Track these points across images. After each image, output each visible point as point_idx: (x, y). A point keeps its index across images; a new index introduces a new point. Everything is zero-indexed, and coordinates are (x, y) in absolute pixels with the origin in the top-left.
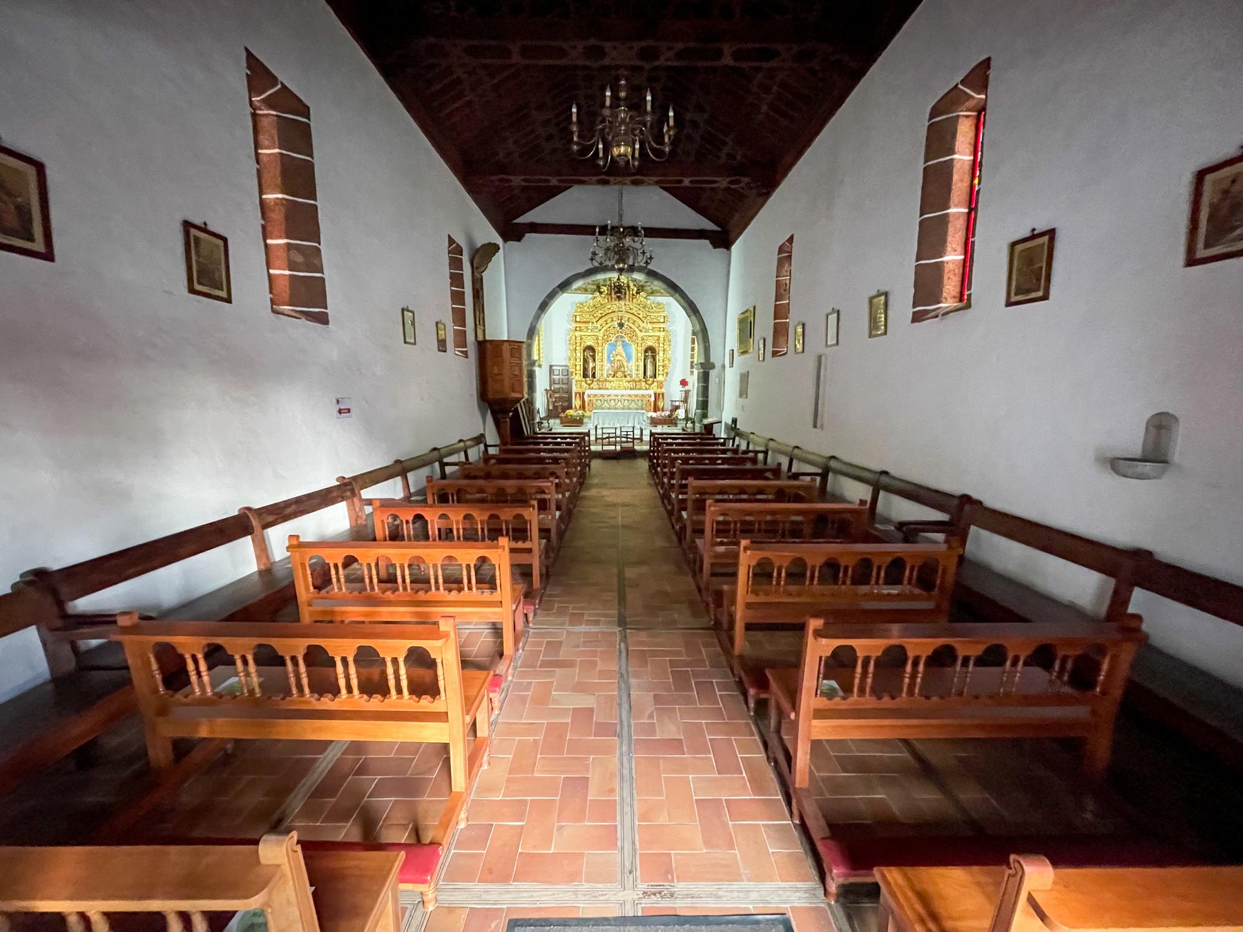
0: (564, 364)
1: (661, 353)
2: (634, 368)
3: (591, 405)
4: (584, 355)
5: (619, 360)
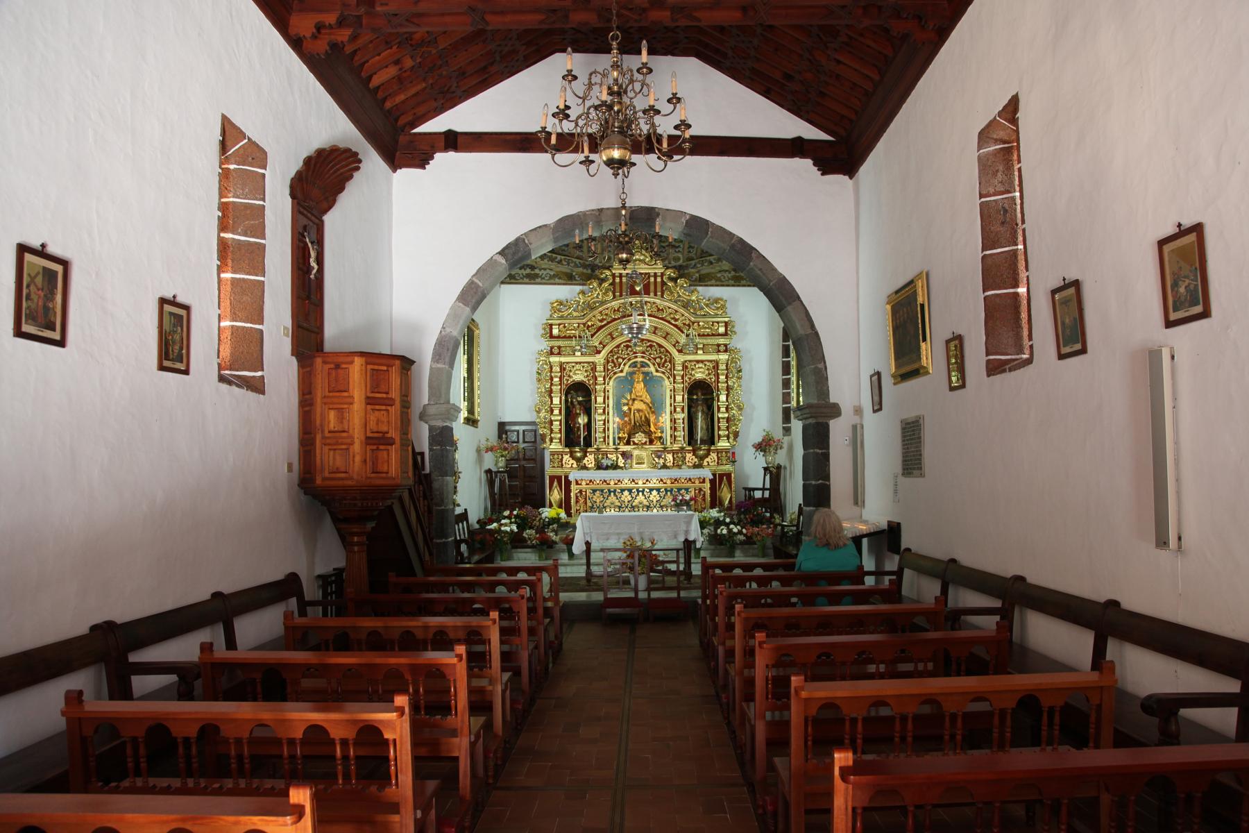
0: (529, 419)
1: (723, 398)
2: (668, 424)
3: (582, 501)
4: (566, 401)
5: (639, 411)
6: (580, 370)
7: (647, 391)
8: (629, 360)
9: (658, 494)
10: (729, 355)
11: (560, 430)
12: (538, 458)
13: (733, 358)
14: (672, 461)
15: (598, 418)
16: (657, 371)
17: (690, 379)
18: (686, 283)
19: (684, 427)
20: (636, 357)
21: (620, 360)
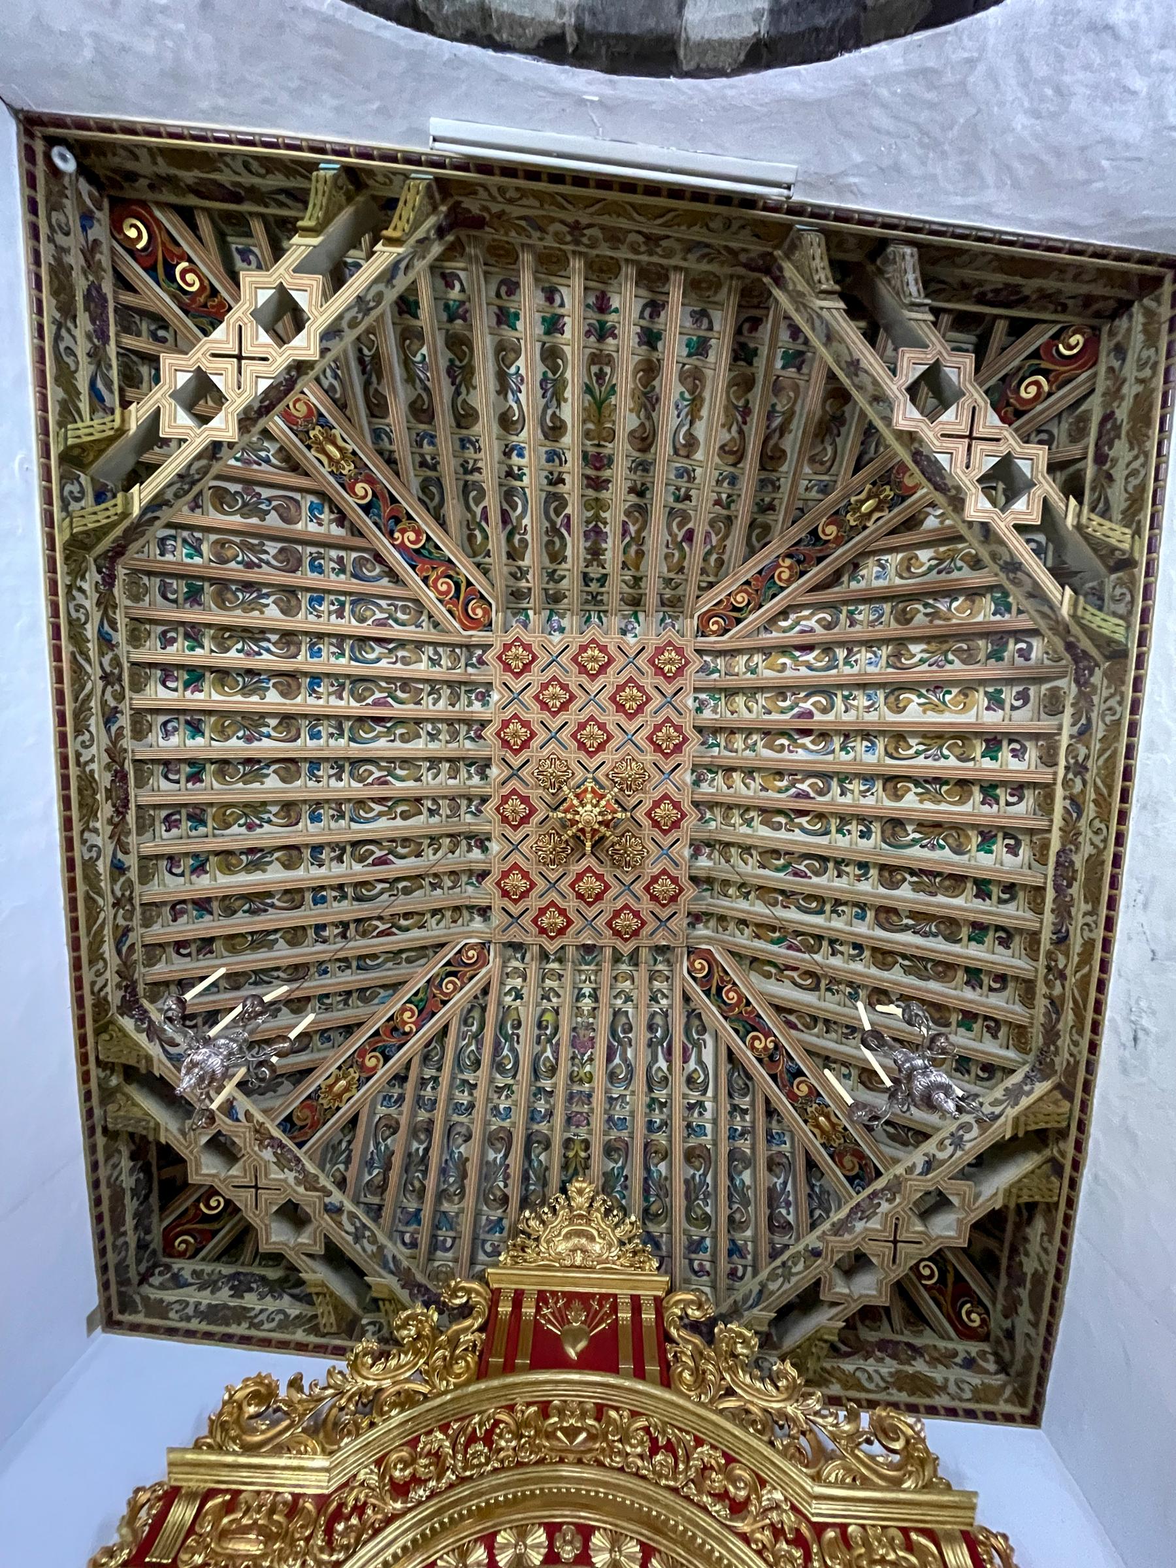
18: (746, 1342)
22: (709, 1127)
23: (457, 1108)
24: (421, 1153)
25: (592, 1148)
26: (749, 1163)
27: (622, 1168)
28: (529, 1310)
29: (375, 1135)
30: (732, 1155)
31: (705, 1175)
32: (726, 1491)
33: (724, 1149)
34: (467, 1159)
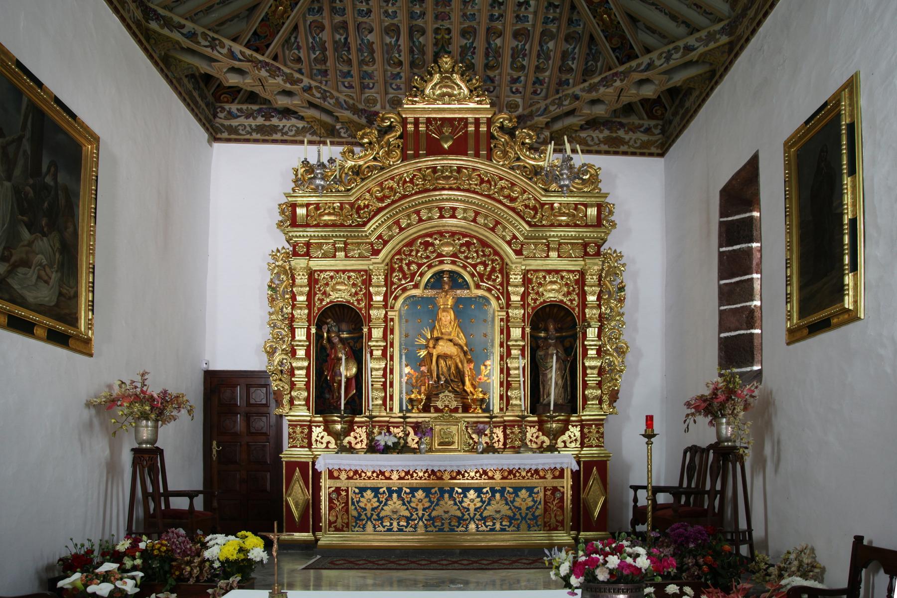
1: (592, 333)
2: (496, 379)
4: (319, 336)
6: (343, 283)
7: (459, 326)
8: (430, 267)
9: (478, 496)
10: (603, 262)
11: (307, 384)
12: (272, 433)
13: (610, 267)
14: (502, 440)
15: (374, 366)
16: (478, 287)
17: (535, 300)
19: (524, 382)
20: (441, 262)
21: (414, 267)
22: (531, 16)
23: (360, 12)
24: (343, 40)
25: (452, 34)
26: (552, 37)
27: (472, 43)
28: (422, 128)
29: (311, 33)
30: (543, 34)
31: (525, 45)
32: (510, 195)
33: (539, 29)
34: (373, 43)
